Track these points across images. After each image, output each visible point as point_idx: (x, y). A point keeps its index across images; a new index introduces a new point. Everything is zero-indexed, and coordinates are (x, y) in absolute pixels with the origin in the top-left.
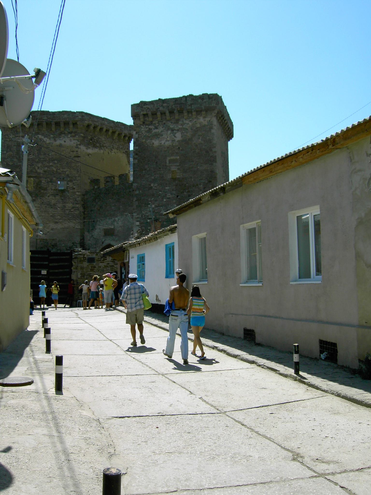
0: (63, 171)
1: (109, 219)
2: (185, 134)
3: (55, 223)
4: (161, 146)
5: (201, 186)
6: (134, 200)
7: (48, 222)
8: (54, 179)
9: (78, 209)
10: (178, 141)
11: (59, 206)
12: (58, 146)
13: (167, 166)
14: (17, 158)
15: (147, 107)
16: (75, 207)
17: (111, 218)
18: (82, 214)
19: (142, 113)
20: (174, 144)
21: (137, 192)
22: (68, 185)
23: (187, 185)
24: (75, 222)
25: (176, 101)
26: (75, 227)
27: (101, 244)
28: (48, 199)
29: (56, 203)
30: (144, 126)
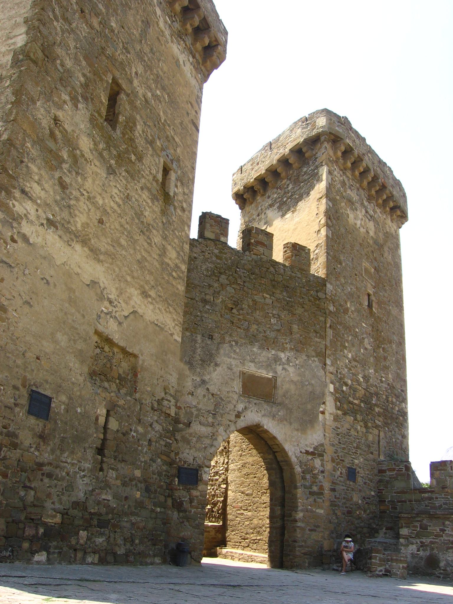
0: (174, 139)
6: (328, 325)
7: (129, 279)
12: (174, 58)
17: (268, 349)
22: (176, 189)
27: (233, 418)
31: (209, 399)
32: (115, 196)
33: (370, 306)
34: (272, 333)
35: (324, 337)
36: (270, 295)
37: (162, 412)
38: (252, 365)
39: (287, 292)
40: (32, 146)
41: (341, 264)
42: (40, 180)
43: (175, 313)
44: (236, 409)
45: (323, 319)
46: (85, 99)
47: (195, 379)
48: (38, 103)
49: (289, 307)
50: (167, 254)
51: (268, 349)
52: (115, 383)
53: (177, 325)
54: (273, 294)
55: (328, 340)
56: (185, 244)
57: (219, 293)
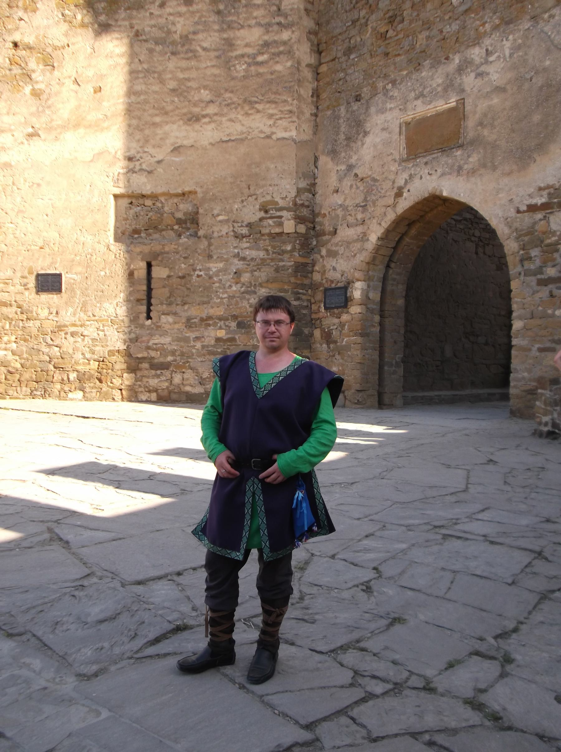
1: (432, 66)
3: (189, 120)
7: (157, 119)
9: (289, 53)
11: (205, 45)
16: (275, 42)
17: (447, 58)
18: (308, 74)
24: (271, 111)
26: (273, 133)
27: (391, 201)
28: (160, 16)
29: (195, 33)
31: (358, 188)
34: (453, 24)
37: (263, 235)
38: (419, 102)
43: (273, 106)
44: (396, 185)
47: (339, 168)
50: (239, 42)
52: (173, 229)
53: (281, 119)
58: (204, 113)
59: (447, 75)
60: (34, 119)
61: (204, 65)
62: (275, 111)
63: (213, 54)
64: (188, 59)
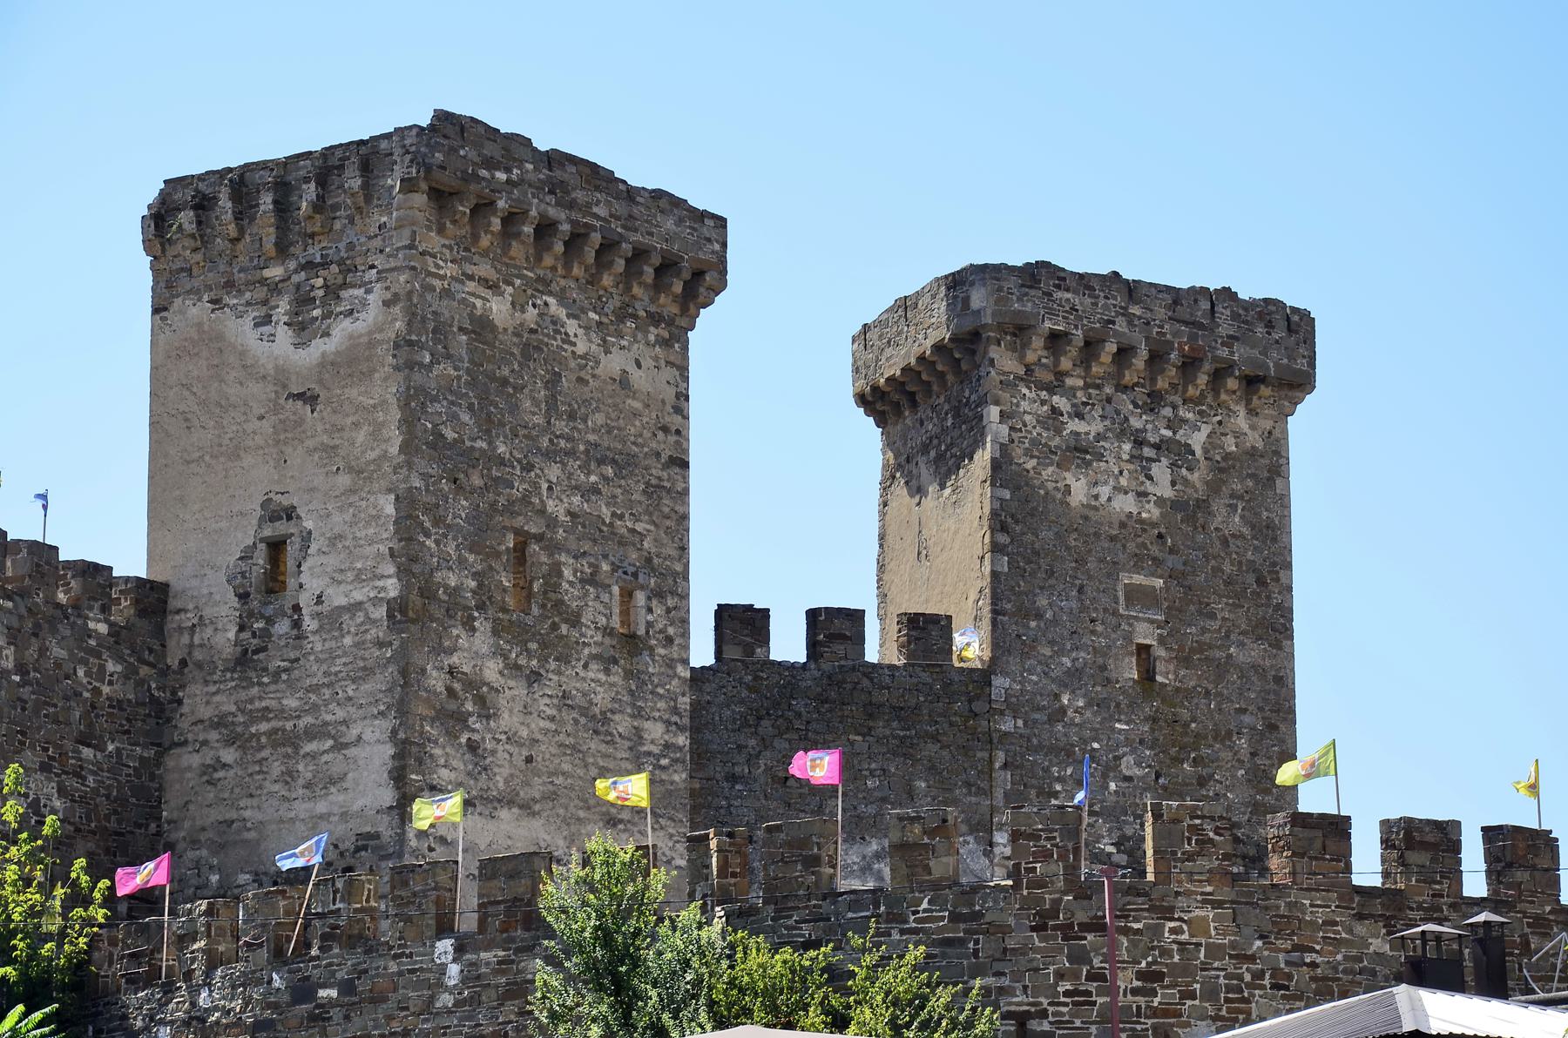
2: (1184, 471)
3: (608, 823)
4: (1096, 508)
5: (1243, 741)
6: (997, 765)
7: (582, 814)
8: (605, 567)
10: (1160, 501)
11: (620, 730)
13: (1122, 616)
14: (470, 407)
15: (1068, 300)
17: (863, 839)
19: (1048, 324)
20: (1144, 515)
21: (1007, 725)
22: (650, 618)
23: (1193, 725)
24: (671, 830)
25: (1176, 302)
30: (1030, 388)
32: (546, 709)
33: (1148, 675)
35: (989, 793)
36: (864, 735)
39: (900, 719)
40: (432, 727)
41: (1039, 616)
42: (446, 761)
43: (673, 825)
45: (986, 755)
46: (481, 607)
48: (429, 667)
49: (905, 749)
50: (646, 736)
51: (863, 839)
53: (678, 842)
54: (867, 732)
55: (999, 794)
56: (681, 699)
57: (758, 756)
58: (620, 817)
59: (864, 857)
60: (472, 782)
61: (619, 756)
62: (674, 832)
63: (627, 744)
64: (608, 743)
